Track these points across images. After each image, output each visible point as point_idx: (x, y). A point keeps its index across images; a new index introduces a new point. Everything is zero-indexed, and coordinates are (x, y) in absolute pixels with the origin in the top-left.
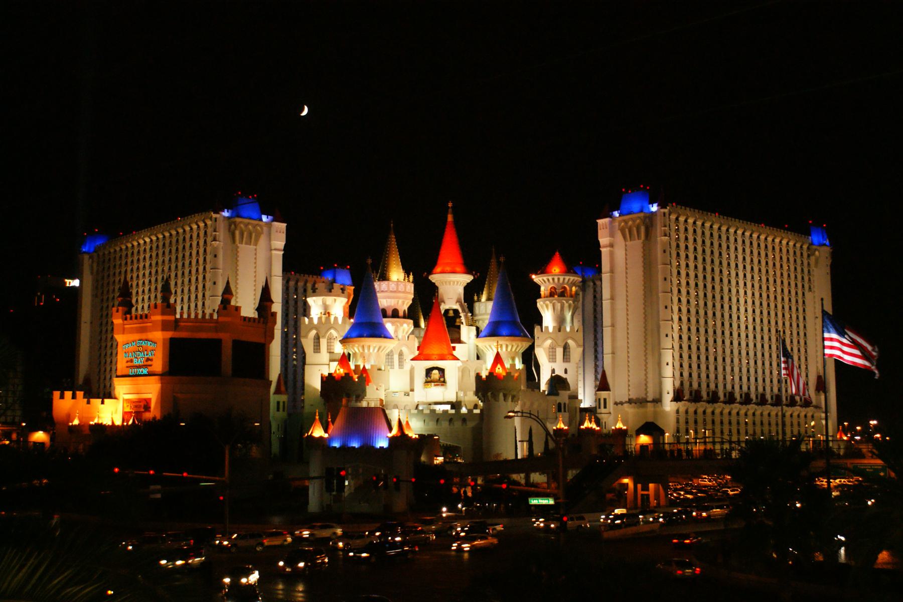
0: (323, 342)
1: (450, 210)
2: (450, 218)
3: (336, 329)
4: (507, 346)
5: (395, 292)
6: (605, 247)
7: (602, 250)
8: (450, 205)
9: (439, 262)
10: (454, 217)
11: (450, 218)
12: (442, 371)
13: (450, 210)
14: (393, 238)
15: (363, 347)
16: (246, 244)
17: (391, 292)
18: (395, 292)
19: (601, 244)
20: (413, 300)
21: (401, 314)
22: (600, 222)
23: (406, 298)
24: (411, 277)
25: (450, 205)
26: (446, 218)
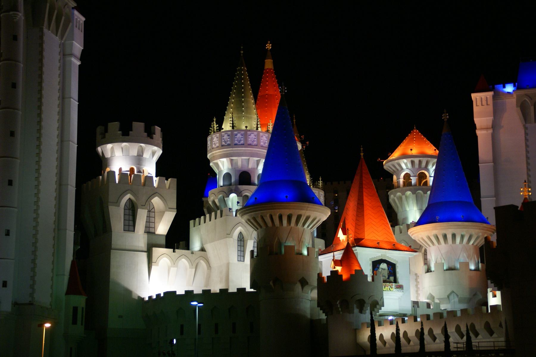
0: (142, 215)
2: (269, 64)
3: (162, 197)
4: (462, 237)
6: (481, 129)
7: (478, 132)
8: (269, 46)
12: (392, 267)
15: (281, 218)
16: (52, 32)
19: (478, 126)
22: (474, 96)
25: (269, 46)
26: (263, 64)
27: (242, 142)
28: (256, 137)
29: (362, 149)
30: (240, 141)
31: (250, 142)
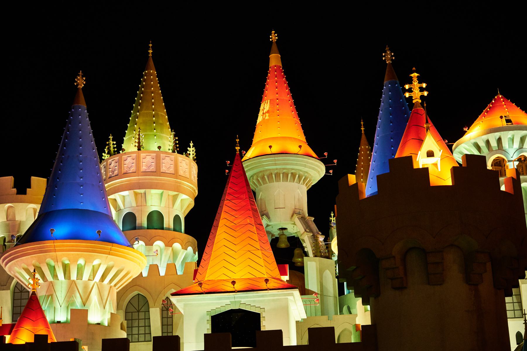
1: (274, 47)
2: (275, 60)
5: (152, 173)
9: (255, 140)
10: (283, 60)
11: (275, 60)
13: (274, 47)
14: (151, 76)
15: (53, 270)
17: (146, 173)
18: (152, 173)
20: (196, 200)
21: (168, 222)
23: (178, 189)
24: (192, 150)
25: (274, 37)
26: (268, 61)
27: (116, 172)
28: (153, 160)
29: (238, 140)
30: (113, 172)
31: (125, 169)
